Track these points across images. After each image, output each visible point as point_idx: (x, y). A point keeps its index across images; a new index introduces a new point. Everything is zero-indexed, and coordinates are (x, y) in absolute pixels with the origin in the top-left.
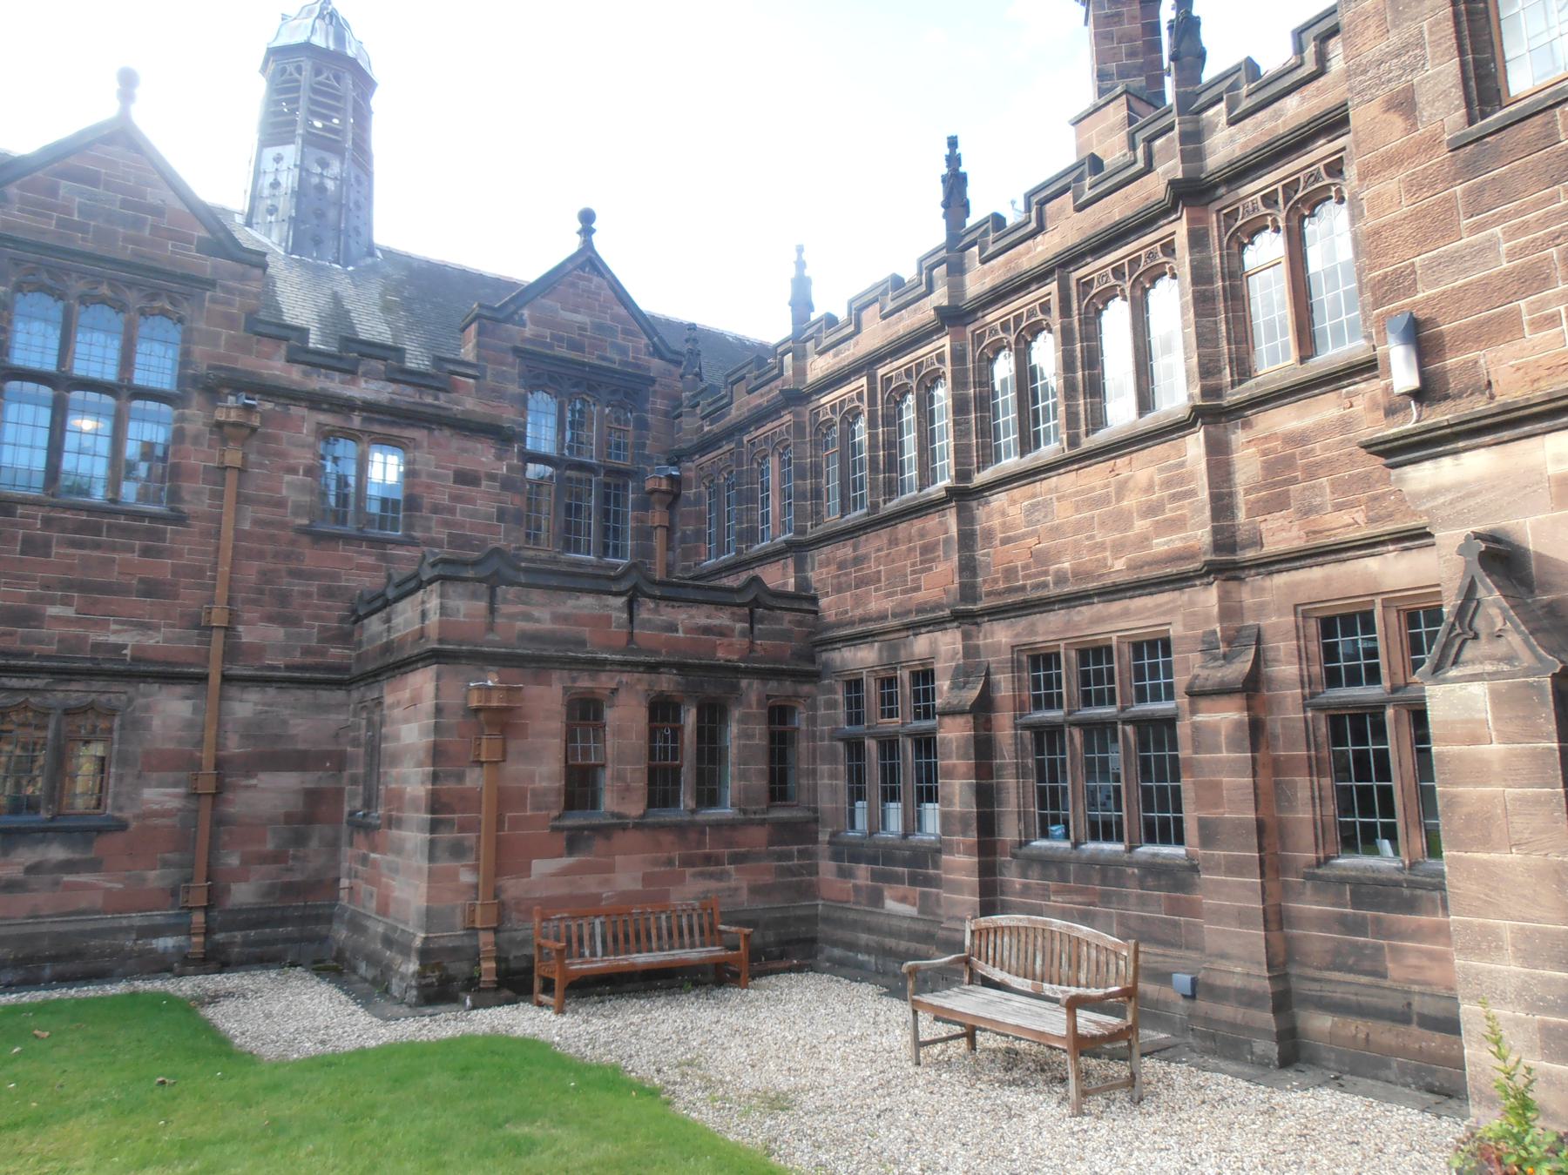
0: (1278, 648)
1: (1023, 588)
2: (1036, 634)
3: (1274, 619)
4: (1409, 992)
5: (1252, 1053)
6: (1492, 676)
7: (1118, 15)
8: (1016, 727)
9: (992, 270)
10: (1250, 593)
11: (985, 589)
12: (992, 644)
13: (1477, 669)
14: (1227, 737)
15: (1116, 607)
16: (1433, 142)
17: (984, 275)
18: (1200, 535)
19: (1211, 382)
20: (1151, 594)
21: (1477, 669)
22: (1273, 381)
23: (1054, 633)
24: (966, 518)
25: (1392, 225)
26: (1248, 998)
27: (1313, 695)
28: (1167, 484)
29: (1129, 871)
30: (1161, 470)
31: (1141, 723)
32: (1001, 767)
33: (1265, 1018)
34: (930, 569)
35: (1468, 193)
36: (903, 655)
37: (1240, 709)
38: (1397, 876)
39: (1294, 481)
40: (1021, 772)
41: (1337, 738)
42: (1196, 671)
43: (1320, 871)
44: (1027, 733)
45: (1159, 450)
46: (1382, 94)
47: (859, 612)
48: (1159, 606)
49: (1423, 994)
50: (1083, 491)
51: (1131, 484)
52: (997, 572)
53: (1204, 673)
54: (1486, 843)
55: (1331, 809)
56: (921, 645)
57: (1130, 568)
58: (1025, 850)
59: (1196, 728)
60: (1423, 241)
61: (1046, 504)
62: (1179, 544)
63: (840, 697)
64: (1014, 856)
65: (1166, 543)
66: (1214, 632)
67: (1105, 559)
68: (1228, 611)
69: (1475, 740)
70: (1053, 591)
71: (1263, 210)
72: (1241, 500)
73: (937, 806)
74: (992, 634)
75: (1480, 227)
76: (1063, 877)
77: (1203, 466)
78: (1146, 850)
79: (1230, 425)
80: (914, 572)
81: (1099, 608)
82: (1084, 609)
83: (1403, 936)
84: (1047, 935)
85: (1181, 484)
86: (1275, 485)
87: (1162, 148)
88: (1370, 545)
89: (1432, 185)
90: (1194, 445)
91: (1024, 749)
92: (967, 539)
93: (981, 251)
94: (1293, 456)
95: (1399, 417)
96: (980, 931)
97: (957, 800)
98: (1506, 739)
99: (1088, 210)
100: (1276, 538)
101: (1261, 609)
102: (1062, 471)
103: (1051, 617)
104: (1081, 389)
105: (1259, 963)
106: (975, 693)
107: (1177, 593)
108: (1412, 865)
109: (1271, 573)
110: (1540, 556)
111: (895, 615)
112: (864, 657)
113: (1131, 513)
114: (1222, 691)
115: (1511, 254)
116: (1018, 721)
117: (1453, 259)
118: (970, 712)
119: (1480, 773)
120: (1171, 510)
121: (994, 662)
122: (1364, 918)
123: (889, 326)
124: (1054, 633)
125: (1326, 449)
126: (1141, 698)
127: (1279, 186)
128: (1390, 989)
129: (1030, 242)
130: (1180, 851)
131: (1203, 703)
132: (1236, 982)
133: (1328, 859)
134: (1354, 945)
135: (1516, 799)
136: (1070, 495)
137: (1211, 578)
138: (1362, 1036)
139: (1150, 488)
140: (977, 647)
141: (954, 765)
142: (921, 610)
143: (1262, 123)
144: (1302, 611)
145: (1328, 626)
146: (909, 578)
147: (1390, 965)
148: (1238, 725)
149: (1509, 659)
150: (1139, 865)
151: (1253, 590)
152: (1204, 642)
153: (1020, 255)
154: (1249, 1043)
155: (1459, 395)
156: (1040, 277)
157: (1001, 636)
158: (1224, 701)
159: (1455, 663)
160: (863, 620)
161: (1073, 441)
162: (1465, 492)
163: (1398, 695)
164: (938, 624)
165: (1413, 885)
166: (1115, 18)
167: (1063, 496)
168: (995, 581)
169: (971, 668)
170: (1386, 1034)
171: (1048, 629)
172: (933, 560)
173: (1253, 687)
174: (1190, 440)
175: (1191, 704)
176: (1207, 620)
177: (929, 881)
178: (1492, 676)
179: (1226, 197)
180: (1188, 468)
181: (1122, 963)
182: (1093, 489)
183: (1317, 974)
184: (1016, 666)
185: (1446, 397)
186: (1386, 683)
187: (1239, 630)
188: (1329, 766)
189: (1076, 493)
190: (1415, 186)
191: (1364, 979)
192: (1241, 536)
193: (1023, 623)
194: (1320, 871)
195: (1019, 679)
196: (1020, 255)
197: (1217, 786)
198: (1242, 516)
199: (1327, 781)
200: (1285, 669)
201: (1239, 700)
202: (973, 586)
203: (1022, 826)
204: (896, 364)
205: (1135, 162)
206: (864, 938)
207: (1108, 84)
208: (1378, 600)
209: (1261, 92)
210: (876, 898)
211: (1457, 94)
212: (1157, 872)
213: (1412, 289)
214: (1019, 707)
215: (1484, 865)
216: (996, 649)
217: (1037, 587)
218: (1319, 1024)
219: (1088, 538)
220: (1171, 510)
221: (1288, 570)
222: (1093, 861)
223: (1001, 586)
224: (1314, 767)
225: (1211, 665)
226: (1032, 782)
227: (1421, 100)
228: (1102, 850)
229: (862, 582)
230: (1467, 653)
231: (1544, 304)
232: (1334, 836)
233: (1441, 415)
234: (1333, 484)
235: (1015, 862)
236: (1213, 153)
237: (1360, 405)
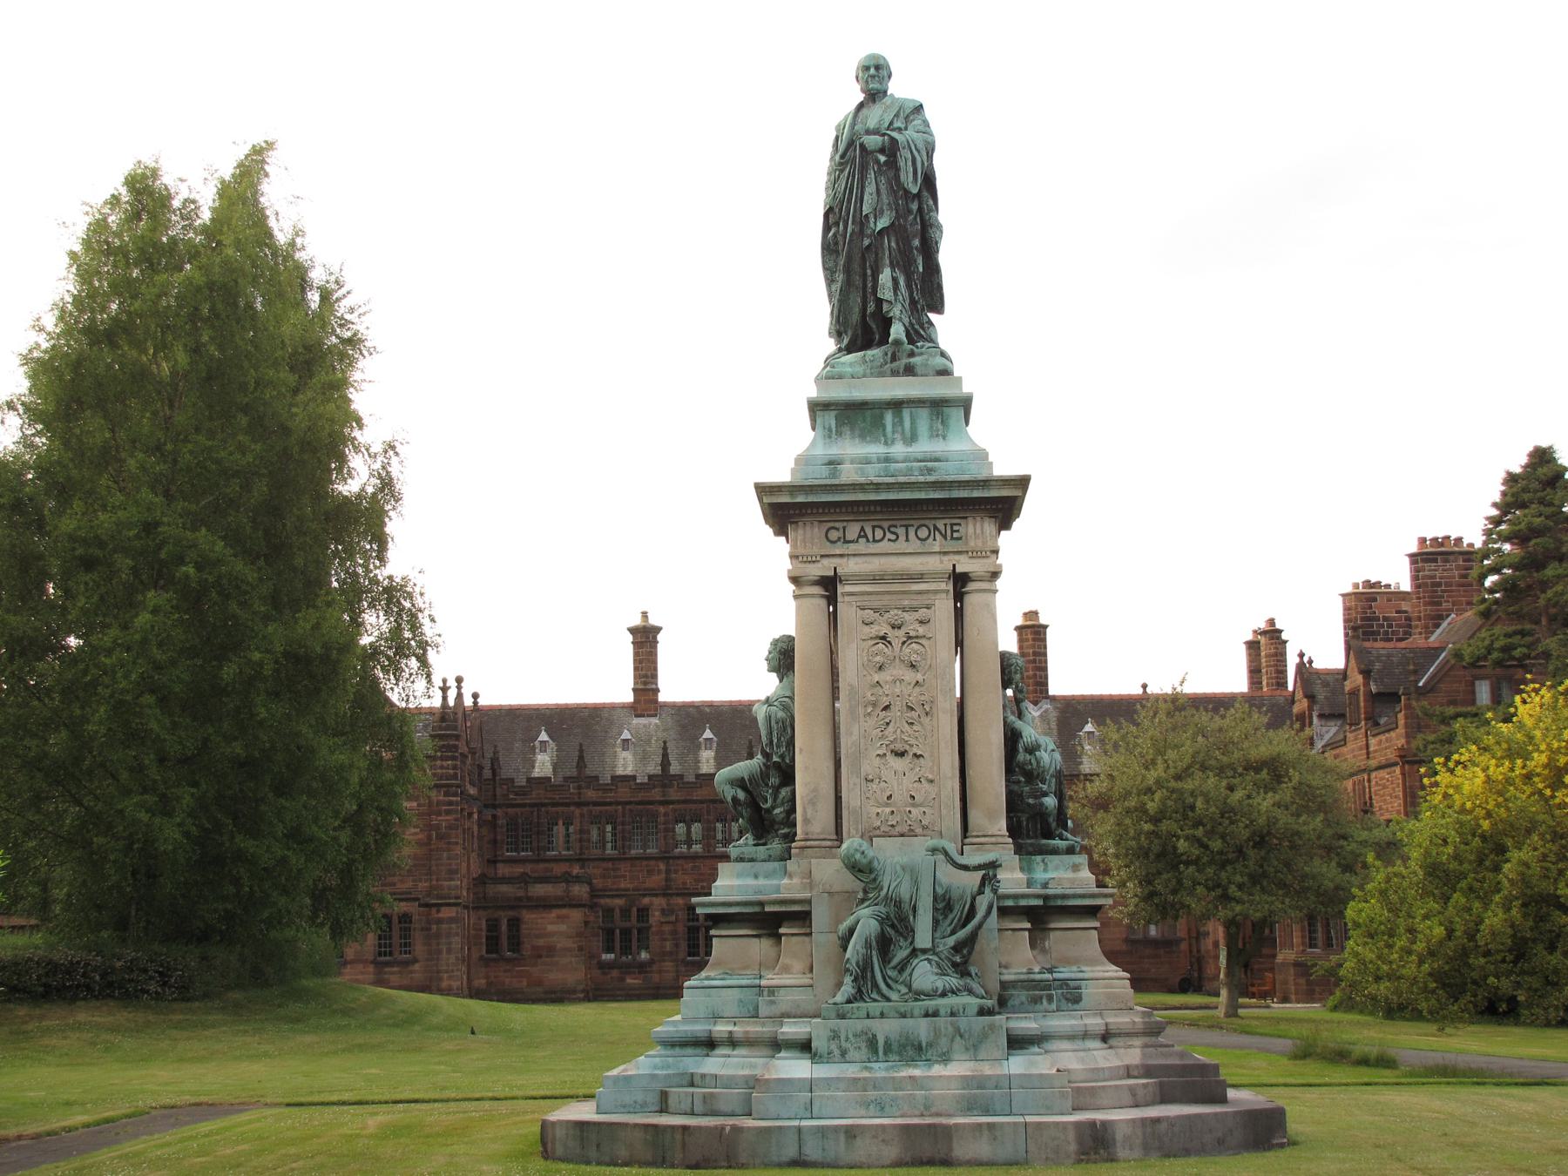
36: (637, 903)
47: (615, 887)
56: (646, 900)
63: (601, 914)
92: (668, 872)
111: (633, 890)
112: (619, 902)
142: (645, 889)
160: (617, 890)
164: (656, 895)
177: (646, 972)
206: (618, 993)
210: (623, 980)
229: (615, 877)
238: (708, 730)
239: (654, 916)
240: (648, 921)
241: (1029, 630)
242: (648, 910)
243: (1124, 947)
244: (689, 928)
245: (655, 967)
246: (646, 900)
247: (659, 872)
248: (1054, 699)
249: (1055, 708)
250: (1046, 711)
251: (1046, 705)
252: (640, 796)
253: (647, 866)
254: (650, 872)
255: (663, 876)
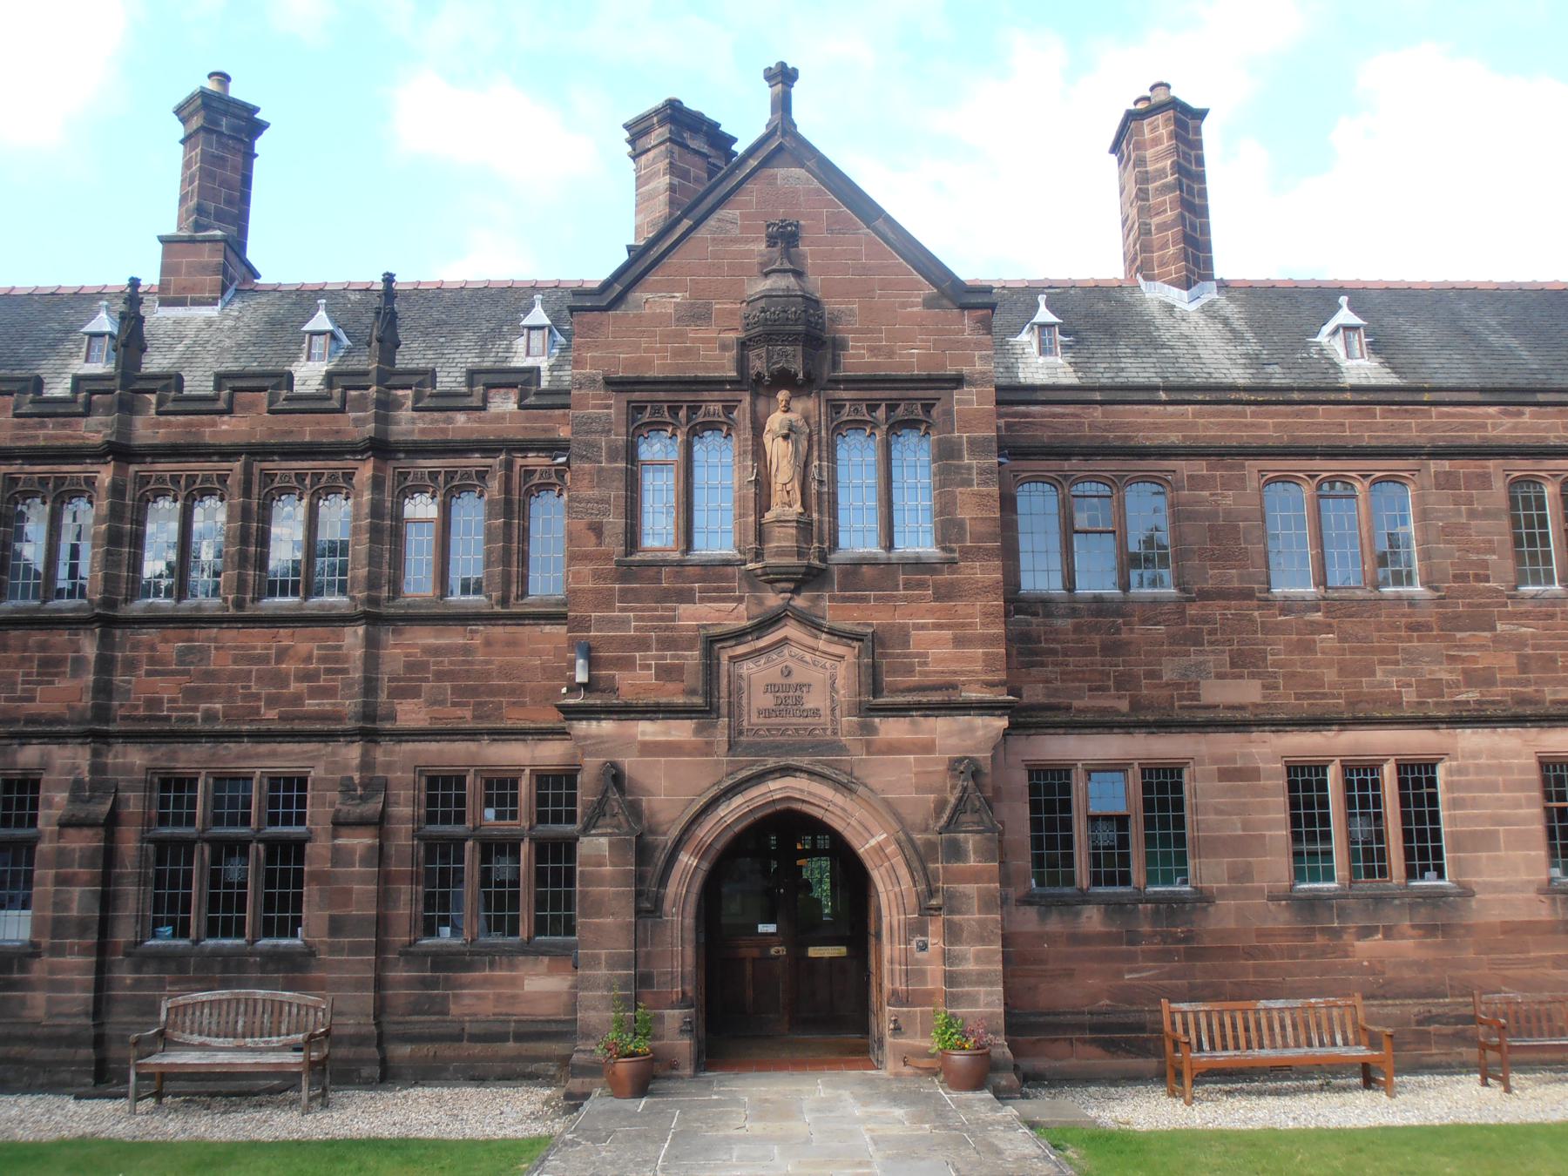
0: (399, 795)
1: (167, 718)
2: (176, 760)
3: (399, 774)
4: (463, 1022)
5: (360, 1077)
6: (611, 835)
7: (223, 159)
8: (142, 840)
9: (168, 425)
10: (381, 753)
11: (121, 712)
12: (124, 764)
13: (604, 831)
14: (361, 856)
15: (264, 748)
16: (607, 557)
17: (158, 425)
18: (350, 705)
19: (374, 594)
20: (299, 742)
21: (604, 831)
22: (421, 607)
23: (197, 762)
24: (106, 643)
25: (583, 591)
26: (358, 1040)
27: (419, 829)
28: (323, 659)
29: (252, 960)
30: (319, 648)
31: (272, 845)
32: (121, 875)
33: (372, 1051)
34: (52, 683)
35: (621, 590)
37: (375, 837)
38: (462, 948)
39: (426, 680)
40: (142, 880)
41: (430, 858)
42: (338, 806)
43: (412, 949)
44: (151, 846)
45: (320, 630)
46: (587, 519)
48: (306, 752)
49: (470, 1021)
50: (243, 647)
51: (291, 652)
52: (139, 699)
53: (345, 809)
54: (599, 914)
55: (421, 906)
56: (29, 755)
57: (282, 718)
58: (139, 949)
59: (336, 850)
60: (596, 608)
61: (203, 651)
62: (328, 708)
64: (127, 955)
65: (318, 705)
66: (351, 778)
67: (259, 708)
68: (366, 765)
69: (600, 865)
70: (199, 726)
71: (429, 483)
72: (385, 685)
73: (29, 912)
74: (125, 755)
75: (623, 610)
76: (182, 969)
77: (359, 652)
78: (265, 943)
79: (383, 629)
80: (24, 682)
81: (247, 746)
82: (232, 745)
83: (462, 986)
84: (251, 1003)
85: (337, 662)
86: (411, 679)
87: (355, 399)
88: (472, 735)
89: (605, 579)
90: (353, 638)
91: (147, 860)
92: (105, 664)
93: (160, 403)
94: (428, 662)
95: (574, 694)
96: (177, 1007)
97: (75, 905)
98: (613, 864)
99: (281, 417)
100: (408, 717)
101: (389, 766)
102: (225, 625)
103: (196, 748)
104: (253, 561)
105: (368, 1015)
106: (107, 807)
107: (322, 745)
108: (473, 940)
109: (401, 741)
110: (630, 778)
113: (288, 675)
114: (361, 823)
115: (637, 629)
116: (146, 835)
117: (611, 620)
118: (102, 825)
119: (600, 880)
120: (325, 680)
121: (123, 780)
122: (438, 977)
123: (23, 426)
124: (197, 762)
125: (451, 663)
126: (273, 820)
127: (443, 470)
128: (451, 1021)
129: (216, 418)
130: (298, 942)
131: (344, 831)
132: (350, 1030)
133: (416, 940)
134: (429, 996)
135: (614, 893)
136: (230, 648)
137: (358, 738)
138: (432, 1054)
139: (308, 659)
140: (106, 764)
141: (75, 874)
142: (32, 720)
143: (437, 421)
144: (419, 770)
145: (432, 782)
146: (20, 687)
147: (452, 1006)
148: (371, 847)
149: (618, 827)
150: (261, 954)
151: (385, 751)
152: (342, 785)
153: (203, 424)
154: (358, 1071)
155: (603, 691)
156: (227, 453)
157: (136, 757)
158: (360, 830)
159: (594, 827)
161: (239, 604)
162: (600, 740)
163: (477, 833)
164: (59, 738)
165: (472, 954)
166: (220, 161)
167: (222, 647)
168: (136, 707)
169: (100, 782)
170: (446, 1050)
171: (187, 758)
172: (56, 675)
173: (380, 823)
174: (348, 630)
175: (334, 830)
176: (346, 767)
178: (611, 835)
179: (403, 462)
180: (345, 651)
181: (320, 1014)
182: (254, 648)
183: (401, 1019)
184: (148, 786)
185: (597, 690)
186: (469, 824)
187: (371, 779)
188: (422, 878)
189: (236, 648)
190: (597, 576)
191: (434, 1018)
192: (381, 711)
193: (163, 749)
194: (412, 949)
195: (150, 797)
196: (203, 424)
197: (349, 892)
198: (383, 697)
199: (420, 888)
200: (403, 810)
201: (373, 830)
202: (108, 708)
203: (139, 928)
204: (27, 468)
205: (330, 398)
207: (204, 220)
208: (472, 770)
209: (440, 399)
211: (622, 537)
212: (278, 959)
213: (588, 629)
214: (147, 822)
215: (597, 925)
216: (128, 769)
217: (182, 720)
218: (401, 1051)
219: (243, 687)
220: (325, 680)
221: (413, 741)
222: (216, 953)
223: (141, 712)
224: (414, 878)
225: (349, 802)
226: (151, 888)
227: (606, 533)
228: (224, 945)
230: (600, 822)
231: (646, 658)
232: (421, 925)
233: (595, 700)
234: (453, 688)
235: (127, 961)
236: (397, 423)
237: (478, 641)
238: (322, 314)
239: (50, 804)
240: (33, 821)
241: (1160, 119)
242: (35, 785)
243: (1543, 912)
244: (162, 844)
245: (39, 969)
246: (29, 755)
247: (79, 663)
248: (1223, 286)
249: (1231, 299)
250: (1212, 304)
251: (1209, 293)
252: (48, 434)
253: (43, 647)
254: (50, 667)
255: (90, 678)
